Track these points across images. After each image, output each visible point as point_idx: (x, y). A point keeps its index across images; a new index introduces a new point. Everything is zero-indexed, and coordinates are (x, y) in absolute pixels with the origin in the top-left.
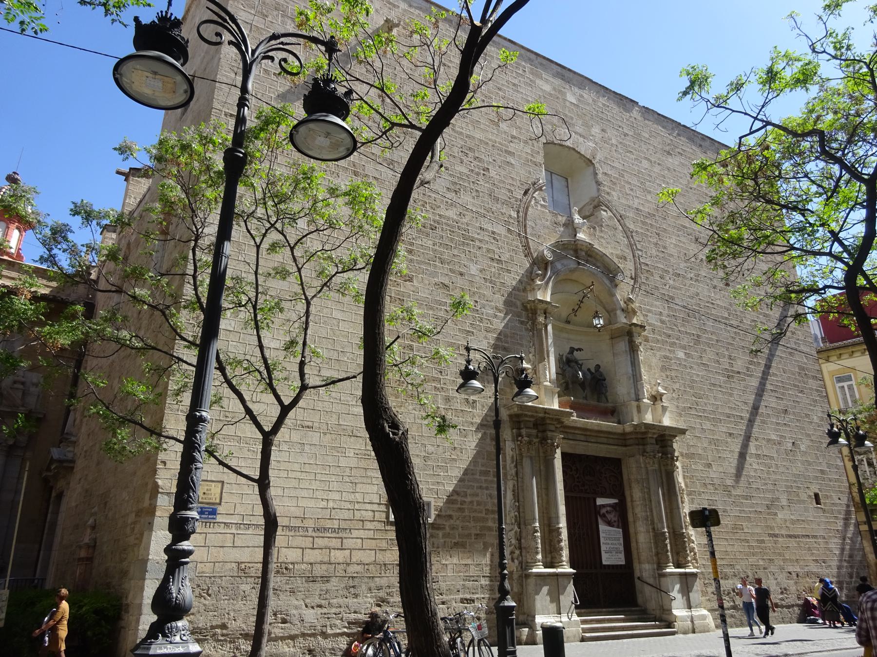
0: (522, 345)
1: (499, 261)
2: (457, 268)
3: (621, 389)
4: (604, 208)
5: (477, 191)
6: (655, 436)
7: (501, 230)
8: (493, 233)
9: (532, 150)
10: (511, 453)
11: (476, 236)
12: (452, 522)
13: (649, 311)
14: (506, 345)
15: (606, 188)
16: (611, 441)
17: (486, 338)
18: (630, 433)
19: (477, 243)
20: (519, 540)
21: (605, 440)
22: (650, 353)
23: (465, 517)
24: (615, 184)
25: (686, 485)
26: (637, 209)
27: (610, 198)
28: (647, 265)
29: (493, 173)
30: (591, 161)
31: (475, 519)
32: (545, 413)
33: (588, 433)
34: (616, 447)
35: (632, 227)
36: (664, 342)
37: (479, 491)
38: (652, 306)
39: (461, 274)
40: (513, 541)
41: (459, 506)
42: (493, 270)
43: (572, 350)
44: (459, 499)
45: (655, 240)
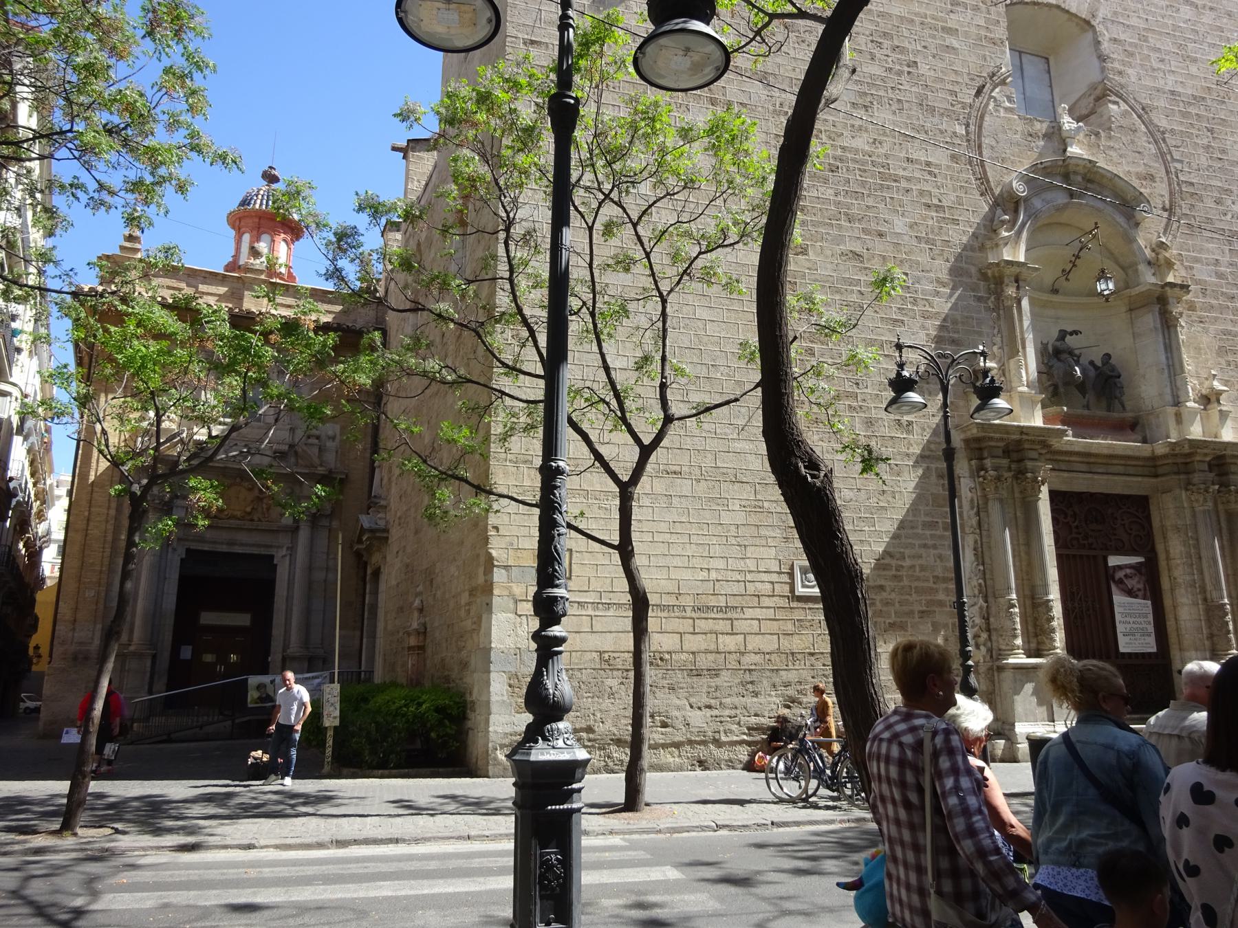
0: (980, 334)
1: (939, 208)
2: (873, 226)
3: (1147, 389)
4: (1113, 98)
5: (899, 101)
6: (1208, 459)
7: (940, 157)
8: (928, 164)
9: (987, 20)
10: (969, 494)
11: (901, 173)
12: (884, 595)
13: (1197, 260)
14: (956, 336)
15: (1116, 65)
16: (1131, 470)
17: (923, 327)
18: (1165, 456)
19: (904, 184)
20: (987, 619)
21: (1121, 469)
22: (1197, 328)
23: (903, 588)
24: (1132, 55)
26: (1173, 93)
27: (1123, 81)
28: (1192, 184)
29: (923, 69)
30: (1088, 23)
31: (918, 591)
32: (1022, 433)
33: (1092, 460)
34: (1140, 479)
35: (1163, 123)
36: (1223, 309)
37: (922, 551)
38: (1201, 251)
39: (881, 235)
40: (978, 620)
41: (894, 572)
42: (930, 222)
43: (1063, 335)
44: (894, 562)
45: (1205, 141)
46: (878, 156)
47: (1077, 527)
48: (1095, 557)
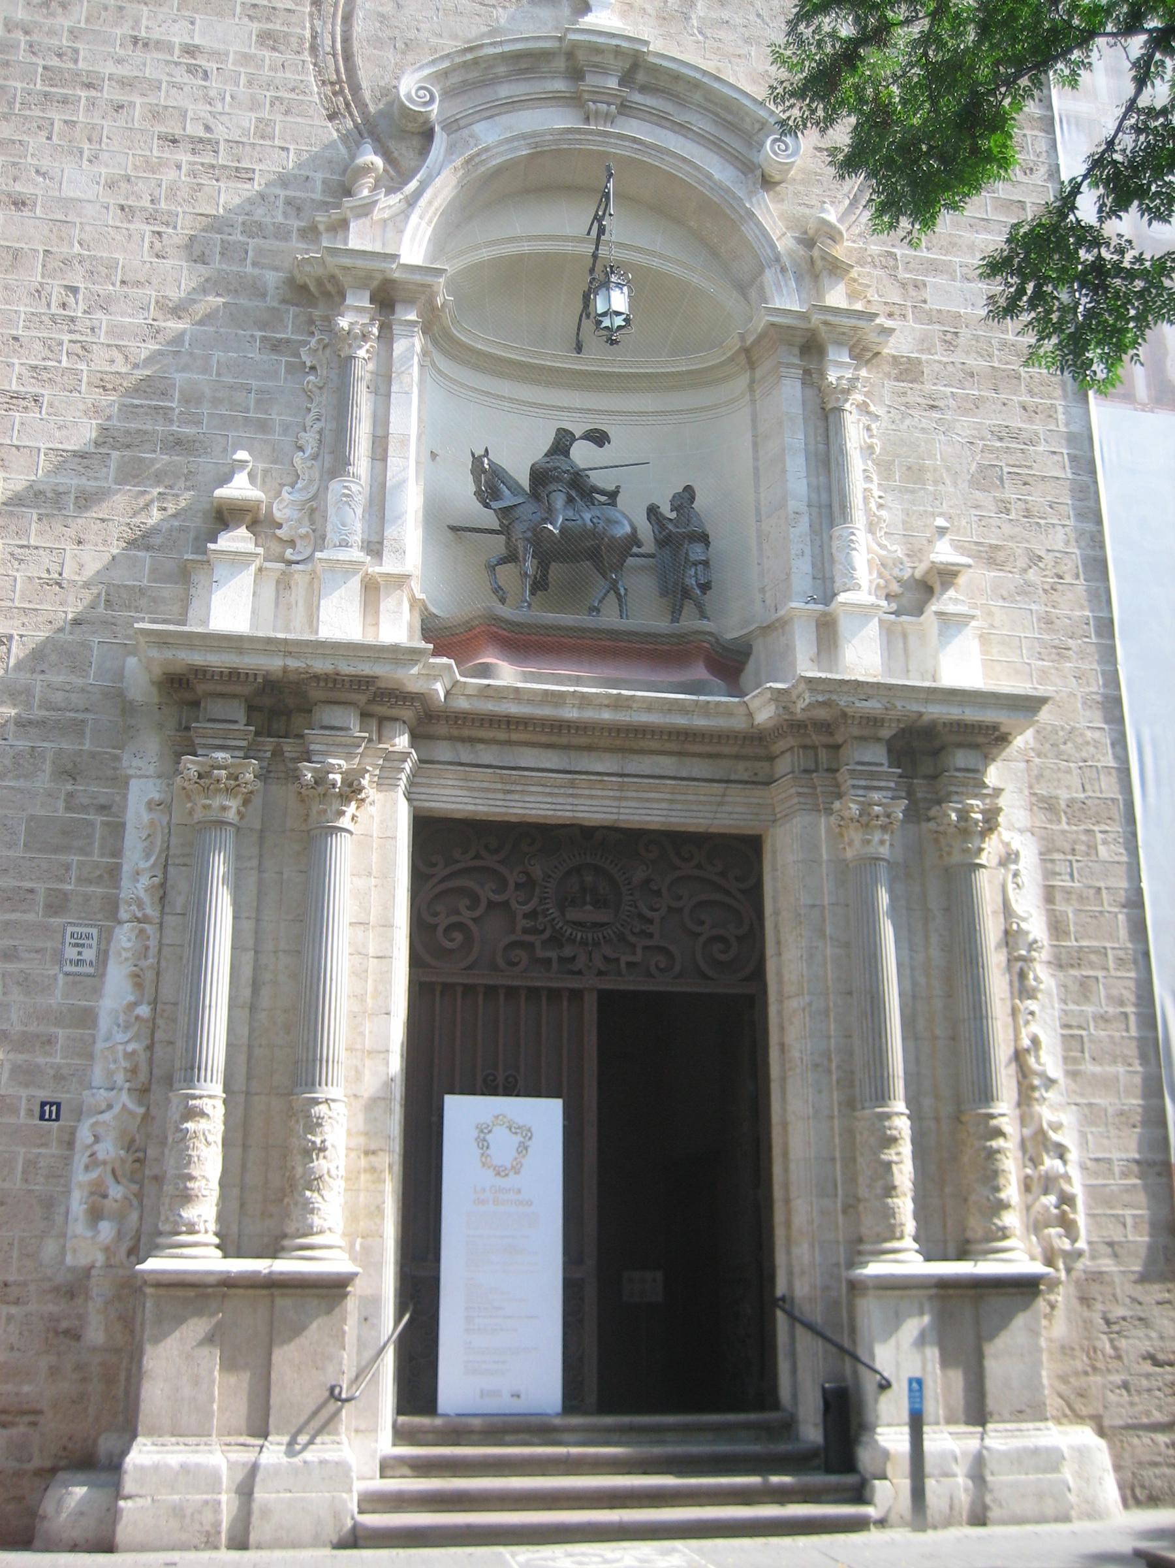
0: (263, 426)
3: (760, 572)
6: (886, 733)
8: (190, 50)
10: (146, 817)
11: (109, 68)
13: (934, 267)
14: (189, 430)
19: (110, 93)
25: (1057, 927)
42: (170, 175)
43: (562, 444)
46: (52, 32)
47: (532, 915)
48: (576, 995)
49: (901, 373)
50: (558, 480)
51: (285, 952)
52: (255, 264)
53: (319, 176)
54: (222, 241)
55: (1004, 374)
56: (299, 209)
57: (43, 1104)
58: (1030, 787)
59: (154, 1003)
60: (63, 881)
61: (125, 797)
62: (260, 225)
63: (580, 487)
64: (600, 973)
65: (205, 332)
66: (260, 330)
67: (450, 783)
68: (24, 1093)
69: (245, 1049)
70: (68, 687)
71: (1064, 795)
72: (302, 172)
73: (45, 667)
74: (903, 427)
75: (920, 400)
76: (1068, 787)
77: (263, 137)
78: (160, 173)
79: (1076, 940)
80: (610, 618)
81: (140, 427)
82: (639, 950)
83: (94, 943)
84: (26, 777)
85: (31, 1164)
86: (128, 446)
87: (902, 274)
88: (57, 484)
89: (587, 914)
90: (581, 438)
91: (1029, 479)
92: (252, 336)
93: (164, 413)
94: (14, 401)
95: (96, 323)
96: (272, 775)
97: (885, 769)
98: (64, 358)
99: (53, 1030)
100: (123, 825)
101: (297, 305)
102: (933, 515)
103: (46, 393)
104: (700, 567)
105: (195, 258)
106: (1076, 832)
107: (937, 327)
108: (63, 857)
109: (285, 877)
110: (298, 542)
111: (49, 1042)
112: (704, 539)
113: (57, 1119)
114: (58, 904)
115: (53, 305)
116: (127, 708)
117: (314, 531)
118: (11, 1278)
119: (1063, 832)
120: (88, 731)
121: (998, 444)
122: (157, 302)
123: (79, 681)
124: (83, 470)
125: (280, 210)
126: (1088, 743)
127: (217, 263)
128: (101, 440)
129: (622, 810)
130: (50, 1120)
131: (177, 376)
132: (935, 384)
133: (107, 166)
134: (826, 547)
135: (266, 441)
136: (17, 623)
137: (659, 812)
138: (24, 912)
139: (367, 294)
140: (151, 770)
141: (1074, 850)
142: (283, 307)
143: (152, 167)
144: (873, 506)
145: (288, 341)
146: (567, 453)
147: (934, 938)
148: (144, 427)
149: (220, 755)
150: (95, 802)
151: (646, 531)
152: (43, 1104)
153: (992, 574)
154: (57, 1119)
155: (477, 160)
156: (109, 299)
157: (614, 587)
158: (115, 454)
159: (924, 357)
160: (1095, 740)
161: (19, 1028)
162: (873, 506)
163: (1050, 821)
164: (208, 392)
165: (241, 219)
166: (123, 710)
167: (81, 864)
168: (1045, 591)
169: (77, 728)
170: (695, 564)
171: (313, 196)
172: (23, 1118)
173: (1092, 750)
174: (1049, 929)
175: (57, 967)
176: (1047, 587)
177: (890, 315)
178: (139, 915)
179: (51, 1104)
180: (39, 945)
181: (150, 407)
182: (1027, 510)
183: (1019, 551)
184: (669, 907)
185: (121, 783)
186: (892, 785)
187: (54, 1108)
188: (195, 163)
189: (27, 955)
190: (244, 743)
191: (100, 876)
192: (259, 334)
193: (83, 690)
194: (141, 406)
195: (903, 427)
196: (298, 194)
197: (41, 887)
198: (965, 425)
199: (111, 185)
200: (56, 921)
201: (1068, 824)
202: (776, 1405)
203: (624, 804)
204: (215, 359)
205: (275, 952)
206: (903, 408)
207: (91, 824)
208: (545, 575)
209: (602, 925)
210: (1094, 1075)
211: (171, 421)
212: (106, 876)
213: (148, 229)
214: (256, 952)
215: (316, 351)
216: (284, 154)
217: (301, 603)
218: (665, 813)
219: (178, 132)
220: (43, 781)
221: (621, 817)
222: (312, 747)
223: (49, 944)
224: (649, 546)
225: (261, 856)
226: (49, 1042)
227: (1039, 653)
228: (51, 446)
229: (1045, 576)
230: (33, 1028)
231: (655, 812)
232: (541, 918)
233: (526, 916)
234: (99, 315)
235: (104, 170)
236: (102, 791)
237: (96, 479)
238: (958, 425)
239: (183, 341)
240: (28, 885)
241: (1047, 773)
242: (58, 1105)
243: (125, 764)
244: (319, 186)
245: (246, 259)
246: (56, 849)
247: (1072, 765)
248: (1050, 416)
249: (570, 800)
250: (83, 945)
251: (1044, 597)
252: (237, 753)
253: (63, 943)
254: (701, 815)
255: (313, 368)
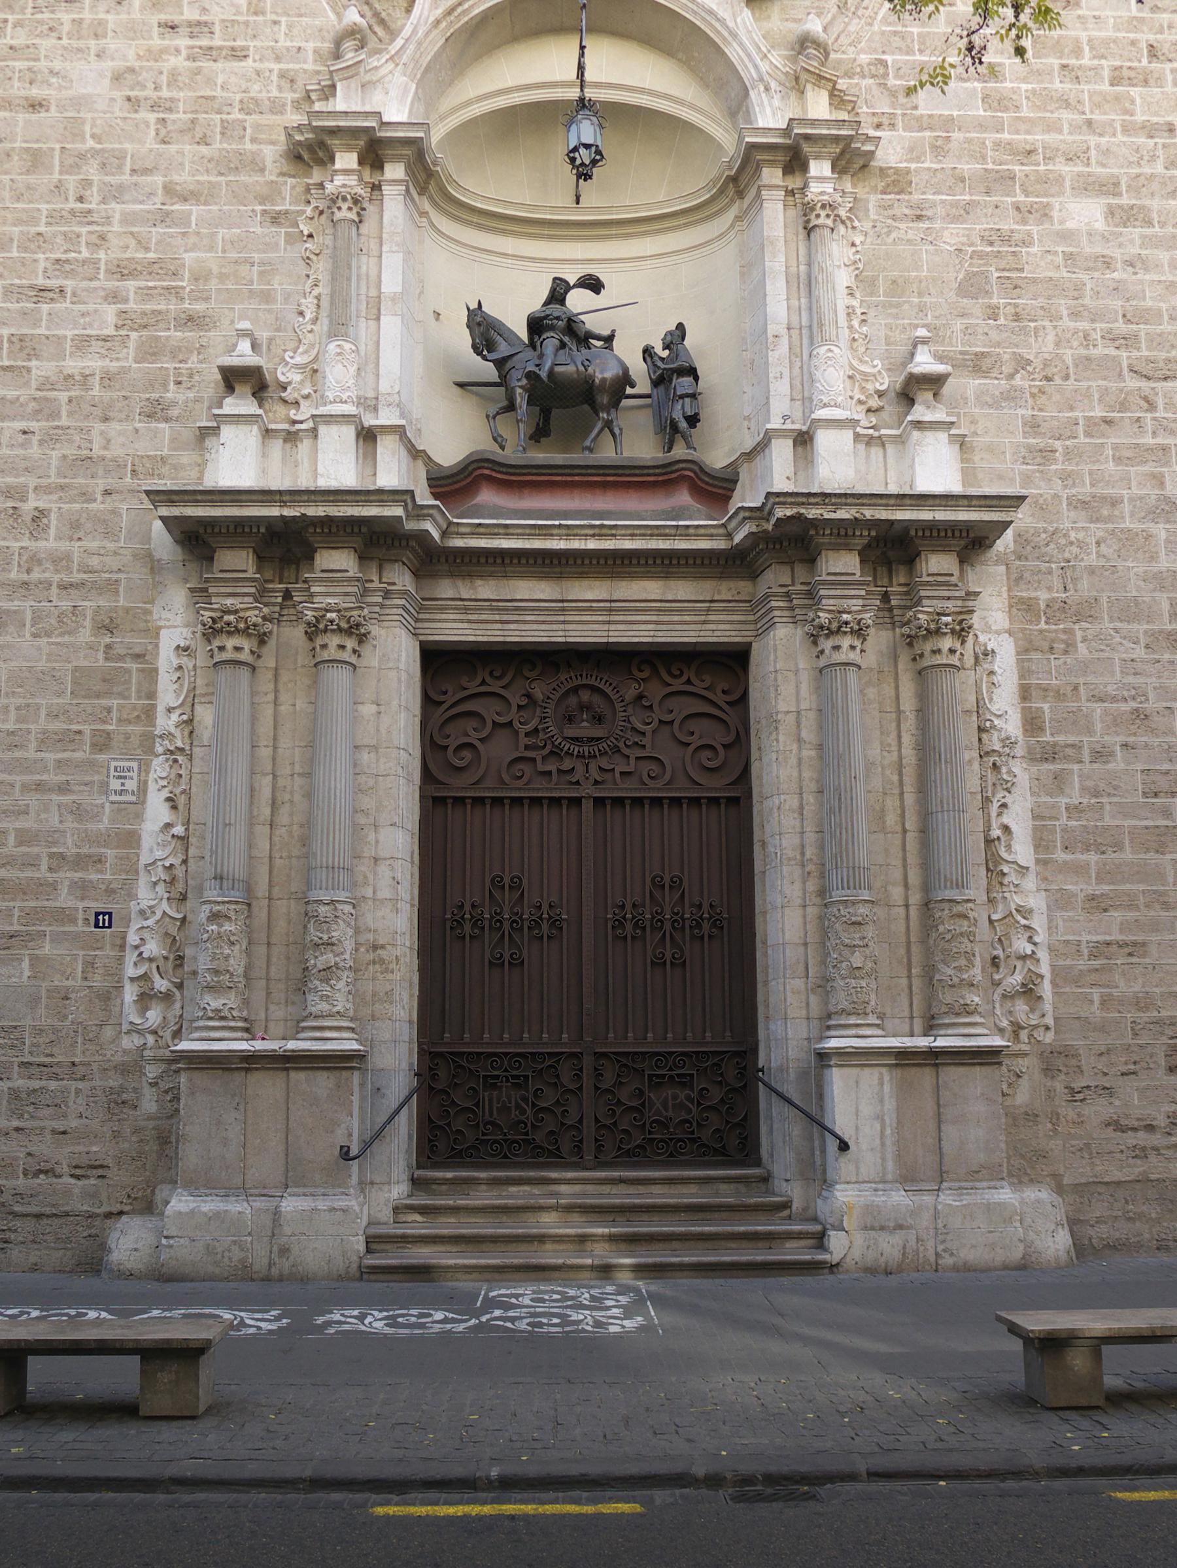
0: (267, 297)
14: (200, 307)
17: (114, 297)
25: (1032, 724)
37: (32, 800)
39: (35, 106)
40: (152, 948)
43: (558, 293)
48: (576, 802)
49: (888, 185)
50: (552, 328)
51: (299, 774)
52: (253, 140)
53: (310, 46)
54: (222, 121)
55: (998, 175)
56: (292, 81)
57: (97, 914)
58: (1009, 590)
59: (187, 823)
60: (105, 722)
61: (157, 646)
62: (256, 101)
63: (576, 334)
64: (596, 782)
65: (209, 211)
66: (260, 204)
67: (452, 617)
68: (81, 905)
69: (266, 860)
70: (102, 552)
71: (1043, 596)
72: (295, 44)
73: (81, 534)
74: (890, 240)
75: (907, 211)
76: (1050, 589)
77: (256, 13)
78: (164, 61)
79: (1052, 735)
80: (607, 453)
81: (155, 307)
82: (632, 761)
83: (135, 775)
84: (69, 633)
85: (90, 964)
86: (145, 327)
87: (892, 82)
88: (84, 368)
89: (585, 728)
90: (575, 286)
91: (1020, 282)
92: (253, 211)
93: (176, 293)
94: (41, 294)
95: (110, 213)
96: (285, 618)
97: (857, 577)
98: (83, 249)
99: (103, 850)
100: (156, 670)
101: (294, 177)
102: (916, 327)
103: (69, 284)
104: (687, 400)
105: (197, 140)
106: (1056, 631)
107: (927, 134)
108: (104, 702)
109: (298, 708)
110: (302, 402)
111: (100, 861)
112: (692, 372)
113: (110, 926)
114: (102, 743)
115: (71, 198)
116: (154, 566)
117: (315, 392)
118: (77, 1060)
119: (1041, 631)
120: (121, 589)
121: (989, 249)
122: (165, 187)
123: (111, 546)
124: (106, 353)
125: (275, 84)
126: (1071, 543)
127: (218, 144)
128: (120, 323)
129: (611, 634)
130: (104, 927)
131: (186, 256)
132: (924, 193)
133: (113, 59)
134: (805, 367)
135: (269, 311)
136: (55, 497)
137: (647, 633)
138: (74, 751)
139: (355, 156)
140: (179, 620)
141: (1052, 648)
142: (281, 179)
143: (157, 55)
144: (856, 323)
145: (287, 212)
146: (562, 302)
147: (907, 739)
148: (159, 307)
149: (229, 601)
150: (130, 652)
151: (638, 368)
152: (97, 914)
153: (977, 382)
154: (110, 926)
155: (460, 10)
156: (121, 188)
157: (608, 425)
158: (134, 335)
159: (913, 166)
160: (1078, 540)
161: (74, 850)
162: (856, 323)
163: (1031, 622)
164: (215, 270)
165: (238, 97)
166: (152, 568)
167: (121, 708)
168: (1033, 395)
169: (112, 587)
170: (682, 397)
171: (306, 67)
172: (80, 927)
173: (1075, 549)
174: (1024, 725)
175: (104, 797)
176: (1035, 391)
177: (878, 126)
178: (172, 748)
179: (104, 914)
180: (87, 778)
181: (163, 288)
182: (1017, 314)
183: (1006, 357)
184: (660, 721)
185: (154, 634)
186: (863, 593)
187: (107, 917)
188: (192, 47)
189: (76, 788)
190: (253, 590)
191: (138, 717)
192: (259, 208)
193: (115, 553)
194: (155, 288)
195: (890, 240)
196: (291, 66)
197: (86, 729)
198: (952, 235)
199: (117, 78)
200: (102, 757)
201: (1047, 623)
202: (758, 1163)
203: (612, 627)
204: (220, 237)
205: (292, 775)
206: (889, 221)
207: (128, 671)
208: (547, 420)
209: (598, 739)
210: (1065, 863)
211: (182, 299)
212: (143, 717)
213: (152, 117)
214: (275, 776)
215: (312, 219)
216: (276, 28)
217: (306, 460)
218: (652, 633)
219: (176, 18)
220: (85, 635)
221: (611, 640)
222: (313, 589)
223: (96, 778)
224: (643, 385)
225: (276, 691)
226: (100, 861)
227: (1024, 458)
228: (76, 332)
229: (1033, 380)
230: (85, 850)
231: (642, 633)
232: (541, 735)
233: (527, 735)
234: (113, 205)
235: (111, 64)
236: (138, 642)
237: (118, 359)
238: (946, 233)
239: (190, 223)
240: (75, 727)
241: (1027, 575)
242: (110, 914)
243: (155, 617)
244: (310, 56)
245: (244, 136)
246: (98, 696)
247: (1053, 566)
248: (1046, 215)
249: (562, 627)
250: (125, 777)
251: (1030, 401)
252: (246, 599)
253: (108, 777)
254: (686, 633)
255: (310, 236)
